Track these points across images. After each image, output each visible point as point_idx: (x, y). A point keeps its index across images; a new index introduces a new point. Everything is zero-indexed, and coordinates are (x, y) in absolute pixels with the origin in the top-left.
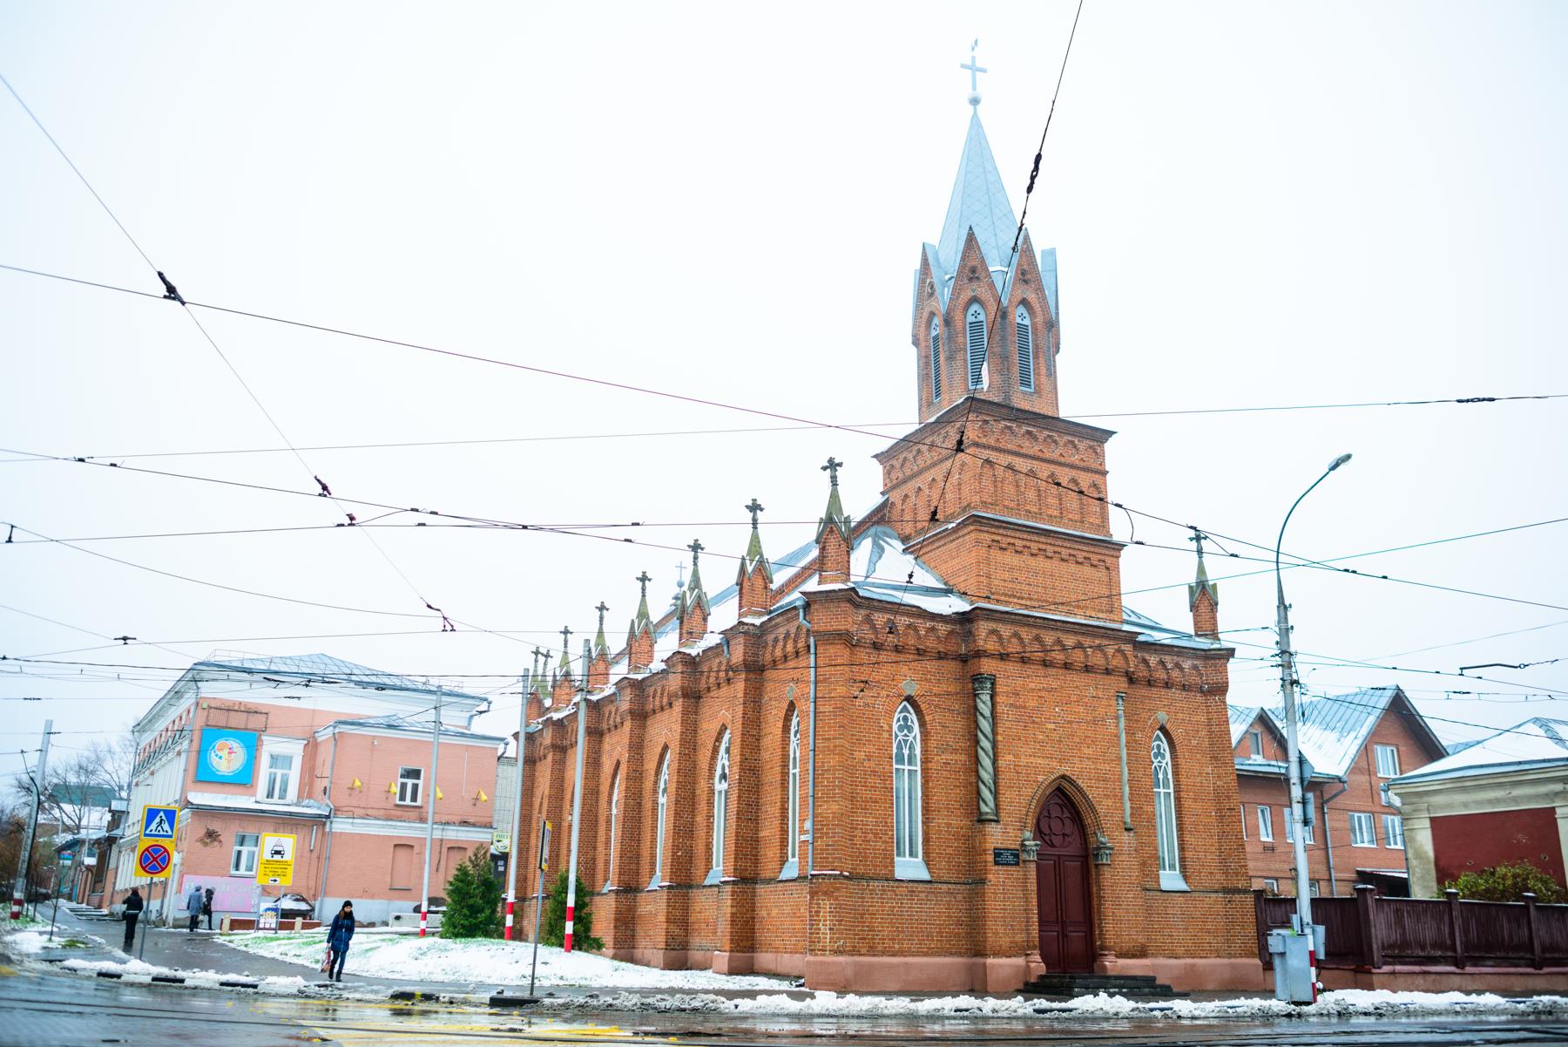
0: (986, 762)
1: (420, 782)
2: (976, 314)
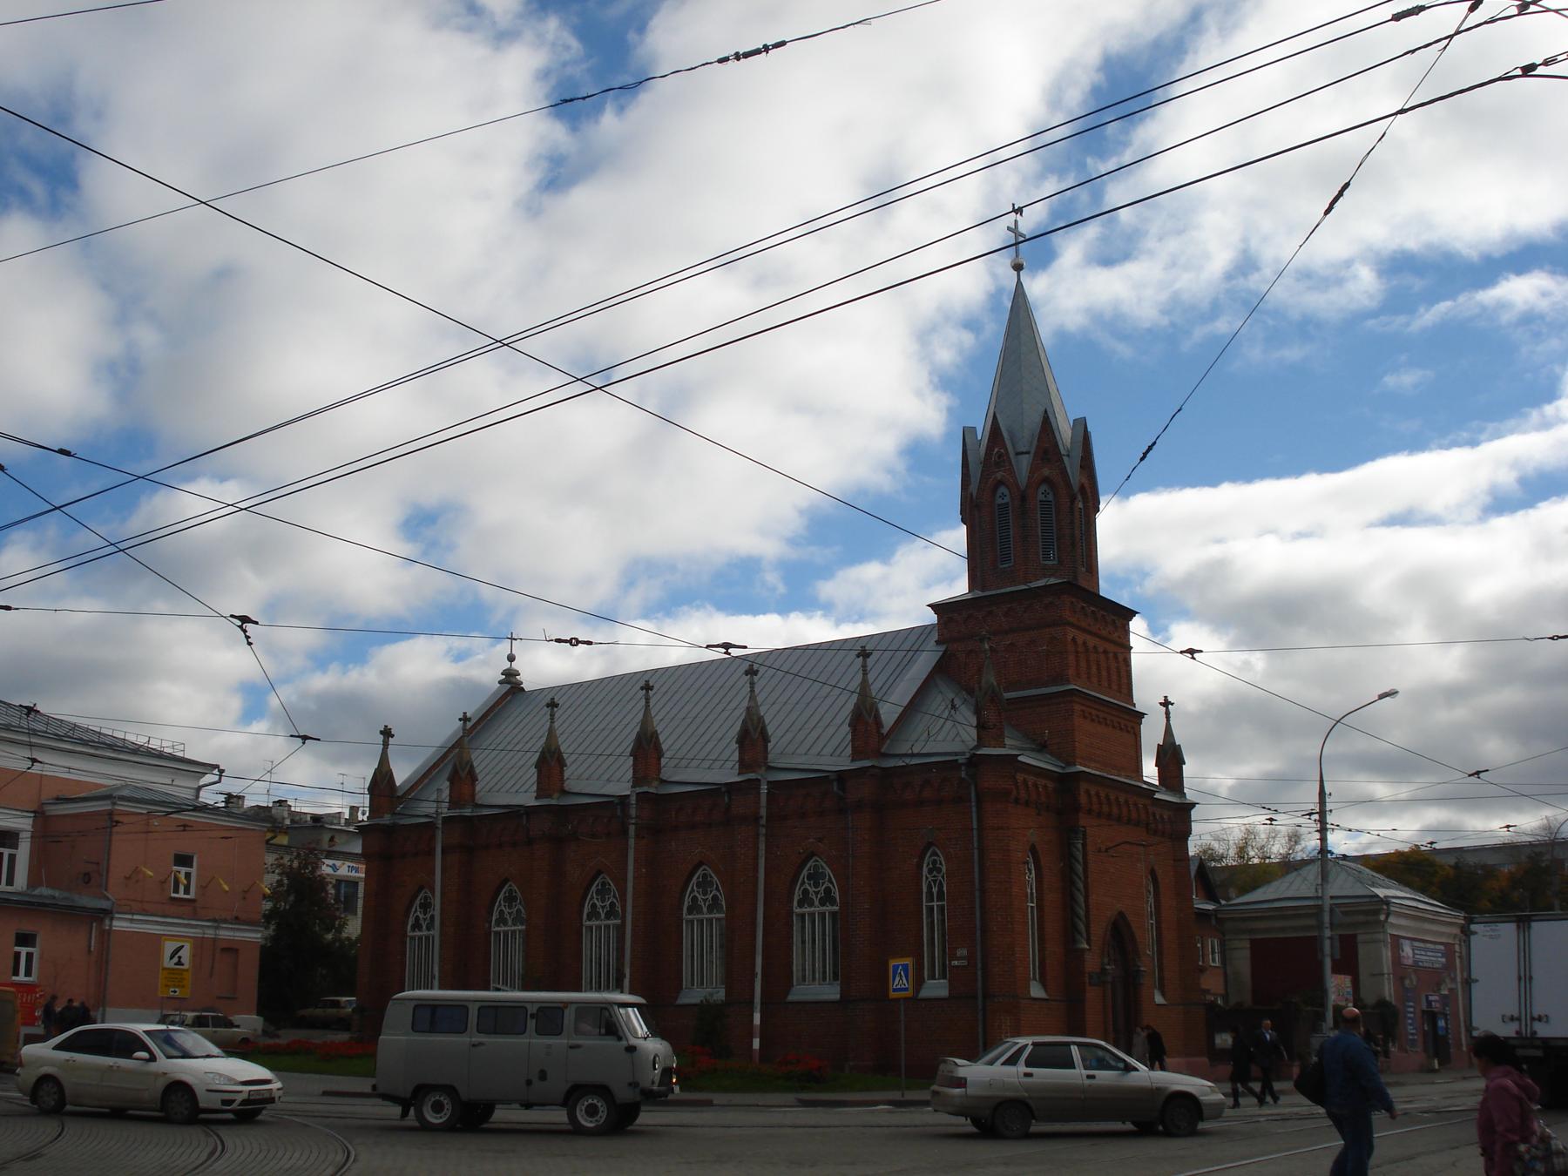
0: (1081, 899)
1: (193, 871)
2: (1045, 493)
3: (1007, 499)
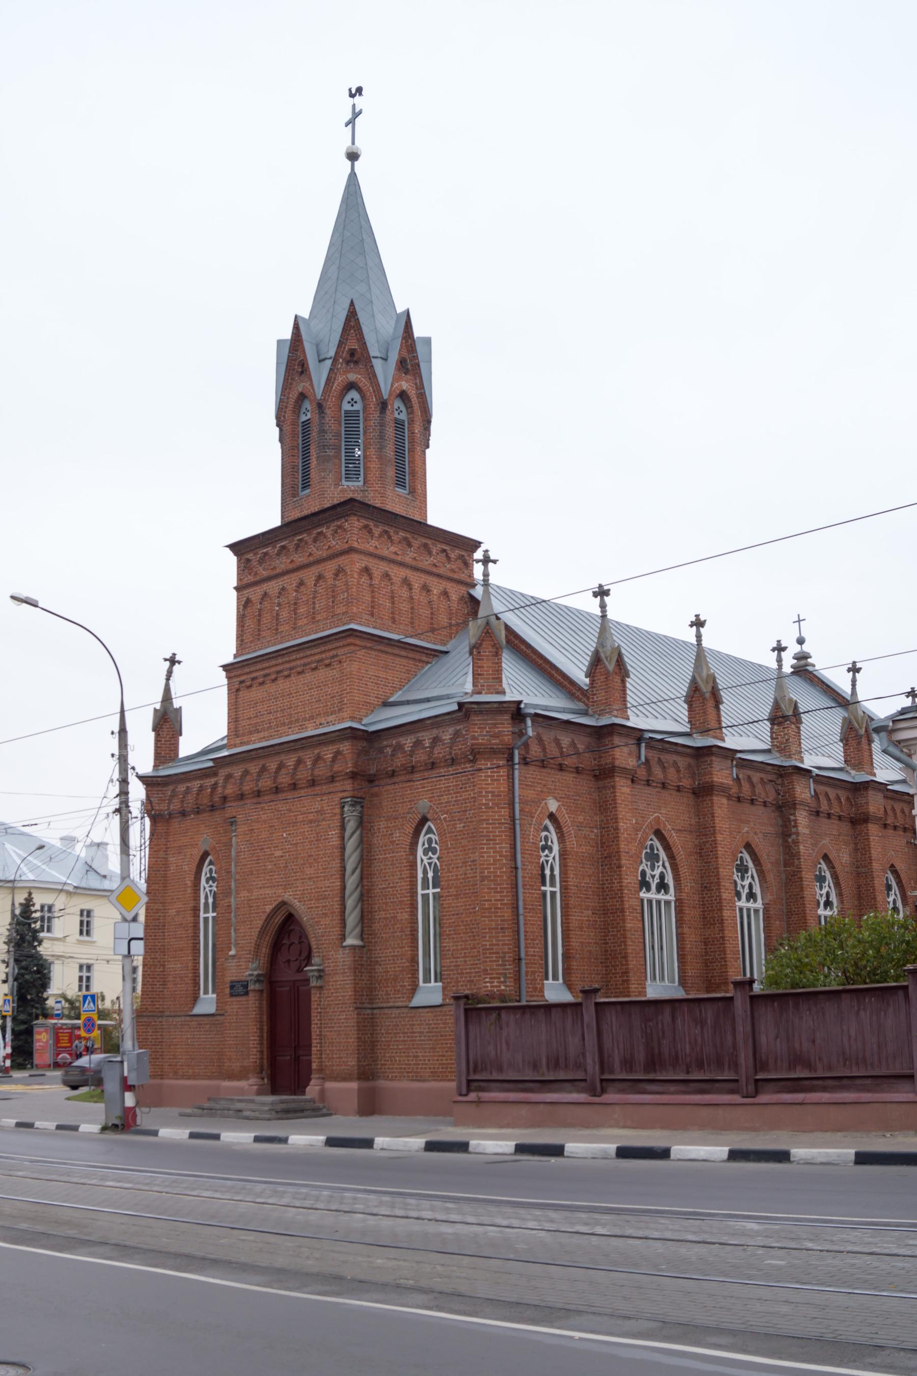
2: (352, 402)
3: (309, 416)
